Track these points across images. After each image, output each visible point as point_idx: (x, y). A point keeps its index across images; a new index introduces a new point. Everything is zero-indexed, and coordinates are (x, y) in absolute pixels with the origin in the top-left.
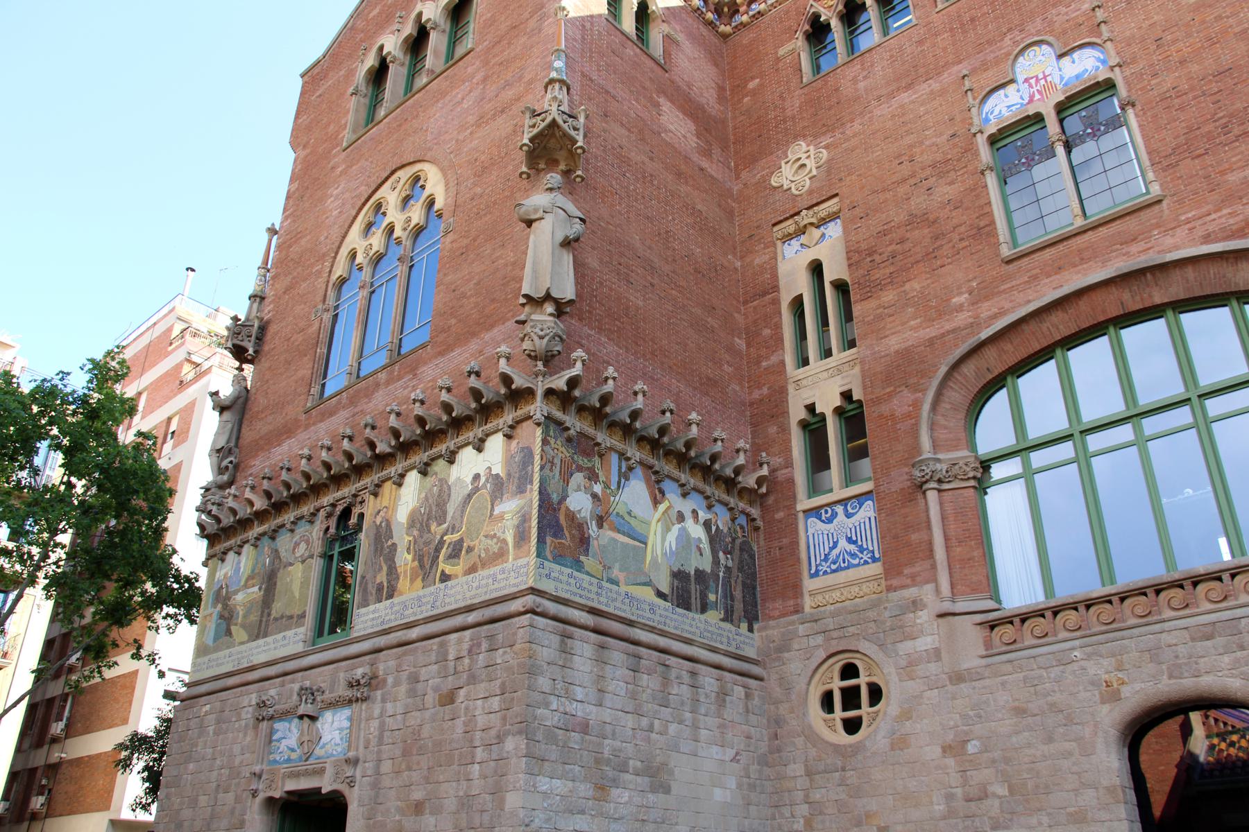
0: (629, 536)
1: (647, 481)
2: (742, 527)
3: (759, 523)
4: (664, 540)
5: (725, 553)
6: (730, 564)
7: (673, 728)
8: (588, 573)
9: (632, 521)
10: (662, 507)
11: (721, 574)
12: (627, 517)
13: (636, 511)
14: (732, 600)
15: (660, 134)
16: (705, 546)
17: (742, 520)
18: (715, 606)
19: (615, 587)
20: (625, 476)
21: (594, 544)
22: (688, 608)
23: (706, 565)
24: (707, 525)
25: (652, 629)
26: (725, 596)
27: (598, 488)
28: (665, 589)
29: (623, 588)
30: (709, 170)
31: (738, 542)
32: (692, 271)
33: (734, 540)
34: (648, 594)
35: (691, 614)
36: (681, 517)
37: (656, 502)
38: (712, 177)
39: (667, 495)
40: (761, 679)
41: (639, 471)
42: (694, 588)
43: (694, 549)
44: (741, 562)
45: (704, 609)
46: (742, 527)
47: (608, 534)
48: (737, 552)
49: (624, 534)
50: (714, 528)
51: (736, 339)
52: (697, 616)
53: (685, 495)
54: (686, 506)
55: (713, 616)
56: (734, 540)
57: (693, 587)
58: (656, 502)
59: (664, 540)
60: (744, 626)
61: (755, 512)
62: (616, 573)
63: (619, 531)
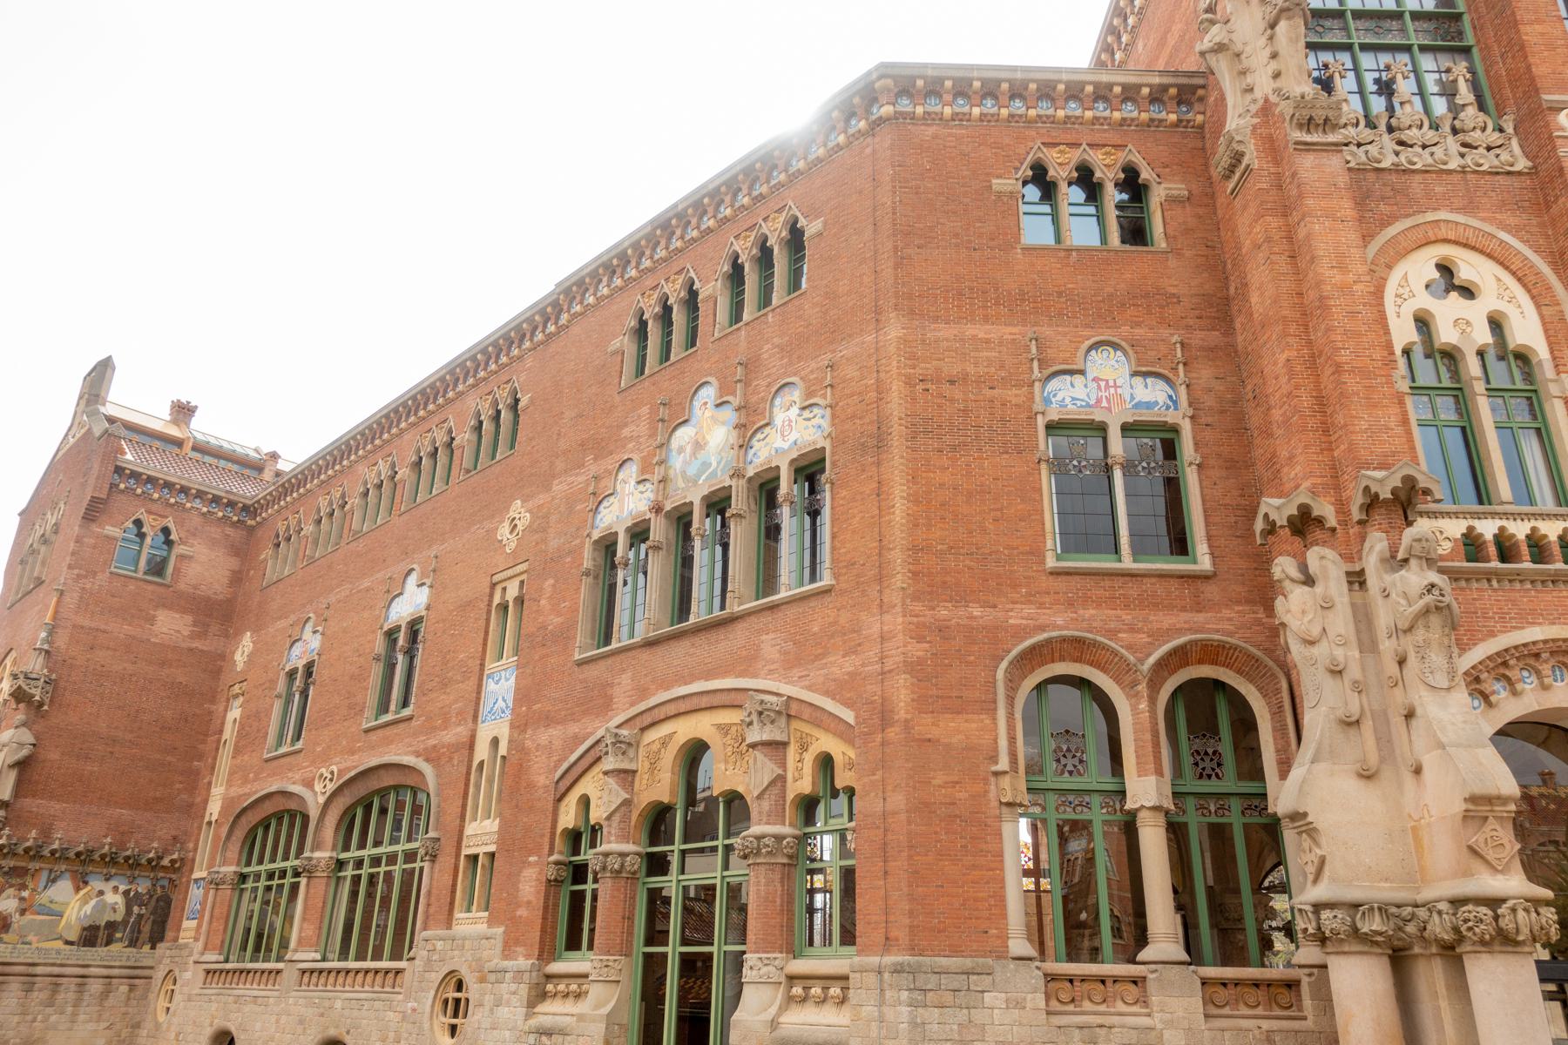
0: (48, 915)
1: (74, 879)
2: (163, 887)
3: (177, 882)
4: (80, 910)
5: (139, 906)
6: (143, 911)
7: (53, 1018)
8: (5, 943)
9: (52, 906)
10: (82, 893)
11: (132, 920)
12: (48, 905)
13: (56, 899)
14: (139, 932)
15: (149, 640)
16: (122, 908)
17: (166, 883)
18: (121, 940)
19: (28, 946)
20: (52, 881)
21: (14, 926)
22: (93, 945)
23: (119, 917)
24: (126, 893)
25: (53, 965)
26: (132, 931)
27: (25, 894)
28: (73, 937)
29: (35, 945)
30: (200, 647)
31: (155, 897)
32: (158, 729)
33: (151, 896)
34: (59, 944)
35: (94, 949)
36: (101, 893)
37: (78, 889)
38: (202, 651)
39: (91, 883)
40: (151, 978)
41: (67, 875)
42: (102, 935)
43: (108, 909)
44: (156, 908)
45: (107, 944)
46: (163, 887)
47: (29, 917)
48: (153, 903)
49: (43, 914)
50: (132, 894)
51: (196, 763)
52: (100, 949)
53: (107, 880)
54: (107, 887)
55: (115, 948)
56: (151, 896)
57: (101, 934)
58: (78, 889)
59: (80, 910)
60: (147, 948)
61: (174, 876)
62: (29, 938)
63: (39, 914)
